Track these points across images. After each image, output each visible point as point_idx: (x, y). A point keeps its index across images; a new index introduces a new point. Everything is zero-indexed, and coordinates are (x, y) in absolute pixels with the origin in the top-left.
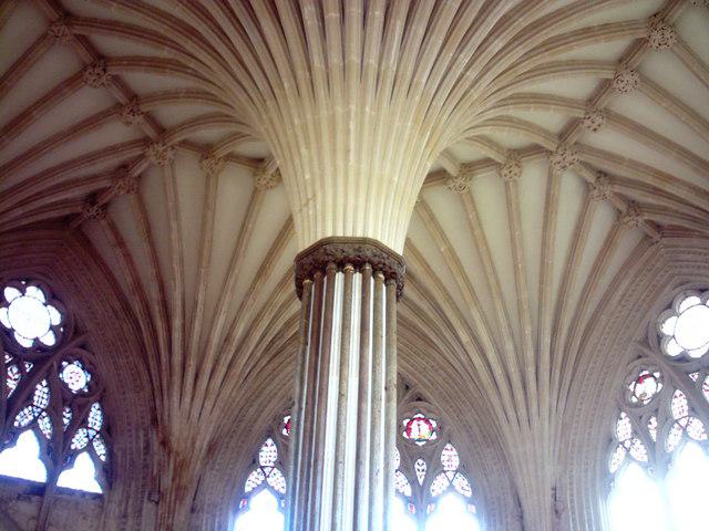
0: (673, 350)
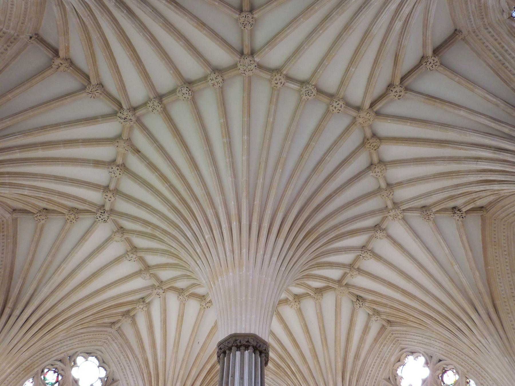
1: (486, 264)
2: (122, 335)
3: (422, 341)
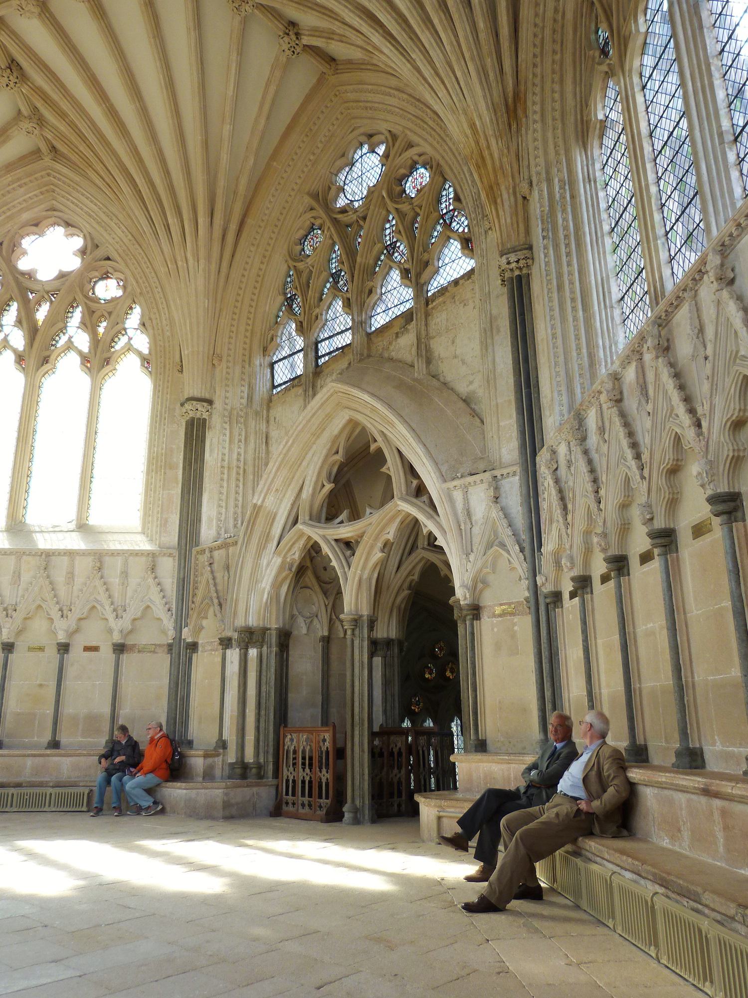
0: (23, 265)
1: (274, 156)
3: (96, 215)
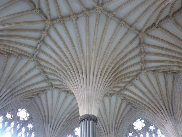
0: (135, 128)
2: (36, 103)
